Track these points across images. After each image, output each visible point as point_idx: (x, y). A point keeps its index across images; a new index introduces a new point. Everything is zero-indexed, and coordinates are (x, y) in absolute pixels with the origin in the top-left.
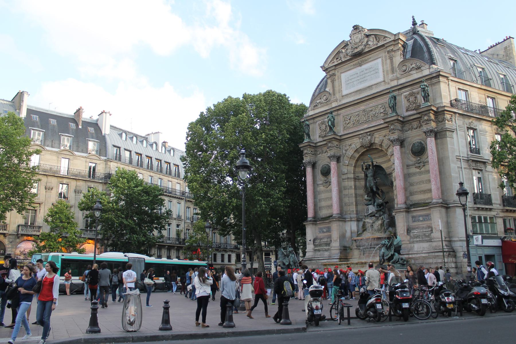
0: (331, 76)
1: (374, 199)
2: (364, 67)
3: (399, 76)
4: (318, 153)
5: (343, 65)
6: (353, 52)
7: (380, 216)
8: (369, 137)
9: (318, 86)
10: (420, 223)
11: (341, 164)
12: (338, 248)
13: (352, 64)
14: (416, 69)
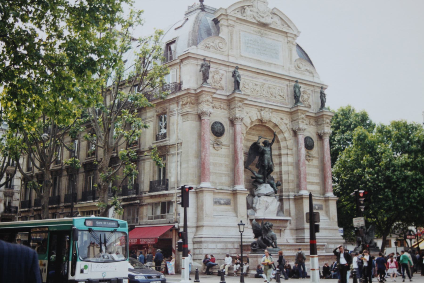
13: (253, 28)
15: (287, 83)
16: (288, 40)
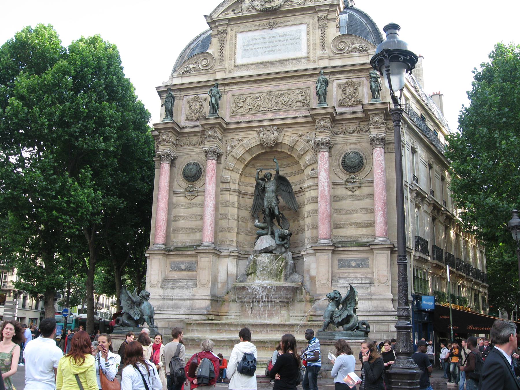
0: (220, 32)
1: (272, 227)
2: (277, 31)
3: (332, 55)
4: (182, 143)
5: (242, 22)
6: (264, 7)
7: (281, 254)
8: (276, 133)
9: (190, 45)
10: (351, 270)
11: (221, 166)
12: (207, 298)
13: (257, 23)
14: (360, 50)
15: (316, 79)
16: (318, 17)
